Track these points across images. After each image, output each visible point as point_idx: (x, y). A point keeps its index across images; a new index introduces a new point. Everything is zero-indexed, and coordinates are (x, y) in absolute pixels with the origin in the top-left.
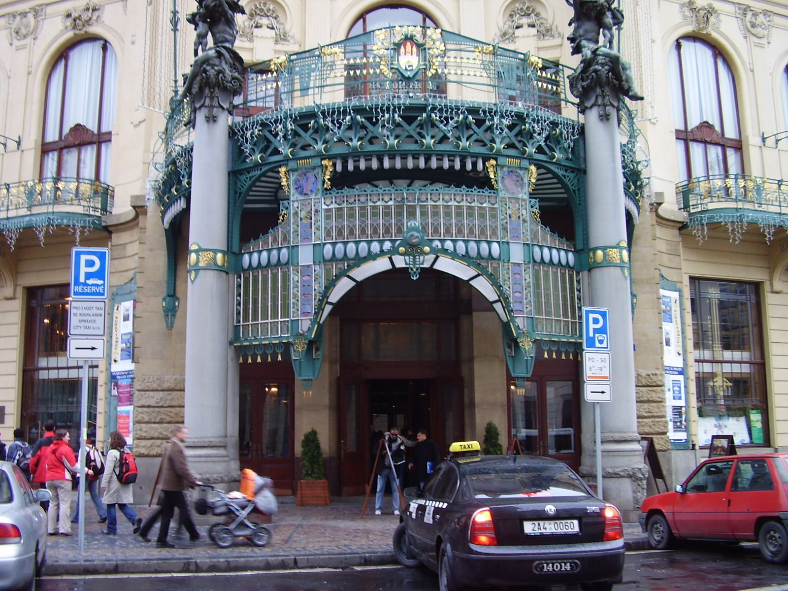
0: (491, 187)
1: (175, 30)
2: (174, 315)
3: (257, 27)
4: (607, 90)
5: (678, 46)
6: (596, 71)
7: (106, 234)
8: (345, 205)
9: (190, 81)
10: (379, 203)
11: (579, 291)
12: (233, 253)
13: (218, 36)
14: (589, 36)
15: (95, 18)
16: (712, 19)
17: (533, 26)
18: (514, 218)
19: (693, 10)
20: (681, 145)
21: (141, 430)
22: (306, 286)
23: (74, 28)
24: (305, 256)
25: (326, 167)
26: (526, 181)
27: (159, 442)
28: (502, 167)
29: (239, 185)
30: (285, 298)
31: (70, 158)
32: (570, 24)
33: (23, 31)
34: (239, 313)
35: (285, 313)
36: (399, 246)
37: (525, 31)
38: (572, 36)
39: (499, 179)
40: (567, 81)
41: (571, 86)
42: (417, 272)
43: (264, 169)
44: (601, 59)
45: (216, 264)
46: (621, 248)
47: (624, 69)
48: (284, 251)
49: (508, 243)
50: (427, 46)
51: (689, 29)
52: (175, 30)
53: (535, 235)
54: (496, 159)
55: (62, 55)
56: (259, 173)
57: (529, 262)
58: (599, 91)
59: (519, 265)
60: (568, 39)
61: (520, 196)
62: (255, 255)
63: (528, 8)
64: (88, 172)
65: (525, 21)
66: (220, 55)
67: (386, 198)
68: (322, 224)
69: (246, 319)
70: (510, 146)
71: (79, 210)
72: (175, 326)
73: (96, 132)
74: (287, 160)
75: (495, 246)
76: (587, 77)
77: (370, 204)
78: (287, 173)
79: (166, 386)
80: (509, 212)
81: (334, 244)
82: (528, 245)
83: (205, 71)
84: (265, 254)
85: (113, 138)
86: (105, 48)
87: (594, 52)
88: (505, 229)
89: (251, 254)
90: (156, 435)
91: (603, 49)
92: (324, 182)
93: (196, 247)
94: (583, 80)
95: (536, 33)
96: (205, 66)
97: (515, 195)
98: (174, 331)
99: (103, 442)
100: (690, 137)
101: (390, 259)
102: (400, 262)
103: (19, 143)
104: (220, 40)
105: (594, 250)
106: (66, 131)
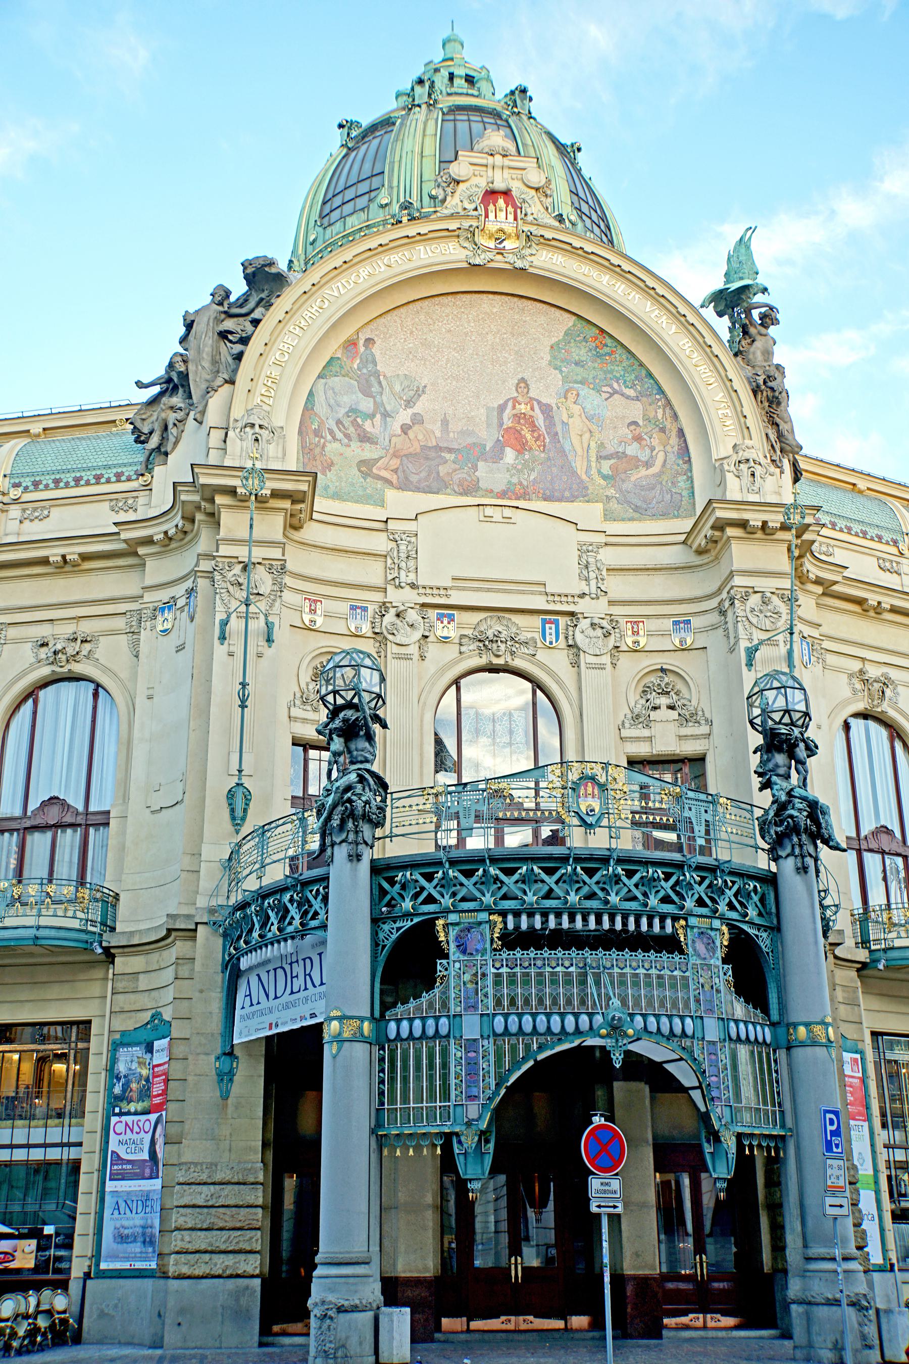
0: (682, 952)
1: (243, 706)
2: (231, 1080)
4: (804, 837)
5: (847, 727)
6: (791, 817)
8: (518, 969)
10: (558, 969)
11: (776, 1072)
12: (379, 1020)
13: (355, 753)
14: (781, 771)
15: (84, 652)
16: (888, 692)
17: (672, 708)
18: (707, 987)
19: (865, 682)
21: (182, 1240)
22: (472, 1066)
24: (471, 1027)
25: (496, 923)
26: (718, 943)
27: (207, 1257)
28: (693, 927)
29: (381, 935)
30: (445, 1077)
31: (39, 843)
32: (755, 752)
34: (381, 1093)
35: (446, 1096)
37: (664, 714)
38: (761, 770)
39: (690, 942)
40: (756, 822)
41: (762, 830)
42: (620, 1058)
43: (416, 920)
46: (827, 1025)
47: (824, 813)
48: (443, 1021)
49: (702, 1018)
50: (609, 787)
51: (860, 706)
52: (243, 706)
54: (686, 919)
55: (31, 694)
56: (409, 924)
57: (725, 1040)
58: (795, 839)
59: (714, 1043)
60: (755, 772)
61: (712, 962)
62: (405, 1024)
64: (66, 867)
65: (664, 701)
66: (361, 779)
68: (490, 991)
69: (393, 1101)
70: (700, 902)
71: (76, 924)
72: (232, 1094)
73: (81, 808)
75: (688, 1021)
76: (782, 822)
77: (548, 969)
78: (446, 926)
79: (218, 1177)
80: (701, 981)
81: (506, 1016)
82: (723, 1019)
83: (350, 801)
85: (112, 822)
86: (96, 695)
87: (789, 794)
88: (698, 1001)
89: (399, 1021)
90: (203, 1247)
91: (798, 789)
93: (339, 1014)
94: (776, 825)
95: (677, 717)
96: (349, 794)
97: (706, 963)
98: (230, 1101)
99: (91, 1259)
100: (864, 846)
102: (590, 1042)
104: (360, 759)
105: (795, 1025)
106: (33, 805)
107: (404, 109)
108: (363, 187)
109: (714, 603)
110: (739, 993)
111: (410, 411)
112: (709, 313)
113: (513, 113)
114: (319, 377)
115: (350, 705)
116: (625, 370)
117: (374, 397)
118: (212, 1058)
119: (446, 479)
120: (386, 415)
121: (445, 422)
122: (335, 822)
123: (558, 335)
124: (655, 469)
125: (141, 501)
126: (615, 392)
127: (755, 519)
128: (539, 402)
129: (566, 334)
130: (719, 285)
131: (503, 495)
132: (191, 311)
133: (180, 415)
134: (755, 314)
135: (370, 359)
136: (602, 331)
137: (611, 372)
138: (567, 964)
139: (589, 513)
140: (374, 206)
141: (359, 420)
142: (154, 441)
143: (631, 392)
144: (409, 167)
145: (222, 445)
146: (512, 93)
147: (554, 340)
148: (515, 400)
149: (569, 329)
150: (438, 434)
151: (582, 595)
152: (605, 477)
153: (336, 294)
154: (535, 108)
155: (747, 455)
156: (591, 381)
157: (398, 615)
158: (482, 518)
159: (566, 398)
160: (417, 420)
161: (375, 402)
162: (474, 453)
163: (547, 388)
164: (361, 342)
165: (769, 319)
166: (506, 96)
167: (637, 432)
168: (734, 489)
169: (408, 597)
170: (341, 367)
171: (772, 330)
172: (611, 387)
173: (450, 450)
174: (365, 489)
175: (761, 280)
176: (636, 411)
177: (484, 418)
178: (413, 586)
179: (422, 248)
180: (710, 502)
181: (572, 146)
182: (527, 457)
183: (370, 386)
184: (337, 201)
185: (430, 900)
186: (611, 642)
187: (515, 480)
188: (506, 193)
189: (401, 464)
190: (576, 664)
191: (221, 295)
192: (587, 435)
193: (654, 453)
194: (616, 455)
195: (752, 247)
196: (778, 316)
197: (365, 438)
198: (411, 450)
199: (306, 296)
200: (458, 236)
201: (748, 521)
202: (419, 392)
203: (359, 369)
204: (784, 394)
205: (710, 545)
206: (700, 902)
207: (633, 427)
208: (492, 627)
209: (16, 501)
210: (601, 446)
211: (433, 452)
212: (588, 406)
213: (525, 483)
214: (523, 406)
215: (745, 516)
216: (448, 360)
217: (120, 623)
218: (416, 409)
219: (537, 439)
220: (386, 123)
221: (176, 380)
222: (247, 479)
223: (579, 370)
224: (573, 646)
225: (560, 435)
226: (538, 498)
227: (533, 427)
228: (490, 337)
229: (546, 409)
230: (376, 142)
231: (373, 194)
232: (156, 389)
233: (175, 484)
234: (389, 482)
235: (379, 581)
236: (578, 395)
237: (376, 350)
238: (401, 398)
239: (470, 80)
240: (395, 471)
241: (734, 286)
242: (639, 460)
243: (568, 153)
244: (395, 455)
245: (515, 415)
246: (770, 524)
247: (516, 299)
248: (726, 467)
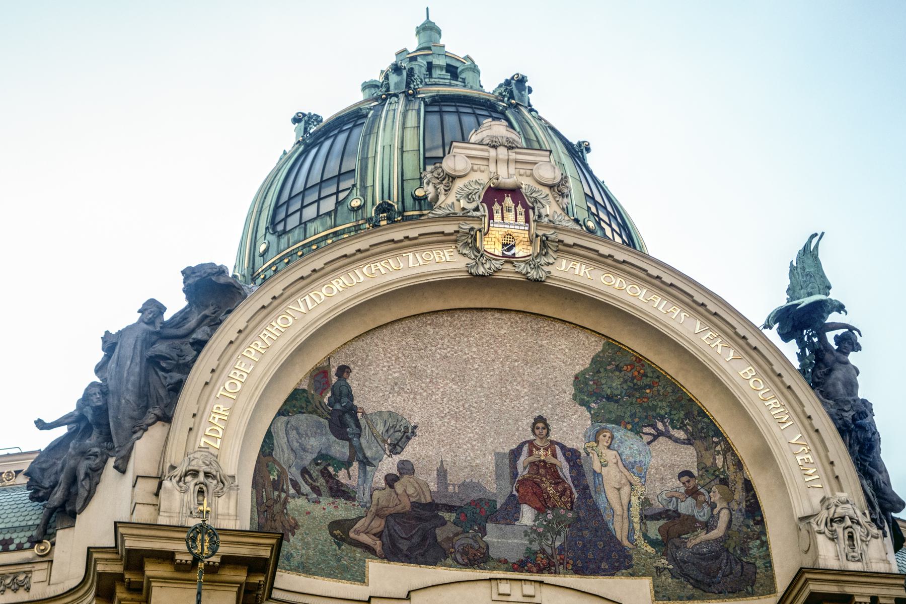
107: (376, 99)
111: (397, 458)
112: (773, 335)
113: (510, 105)
114: (281, 413)
116: (671, 406)
117: (349, 440)
119: (445, 546)
120: (365, 462)
121: (442, 473)
123: (582, 363)
124: (718, 532)
125: (39, 574)
126: (660, 434)
128: (563, 447)
129: (594, 361)
130: (781, 301)
131: (520, 566)
132: (113, 331)
133: (94, 462)
134: (830, 336)
135: (345, 391)
136: (640, 360)
137: (654, 408)
140: (343, 210)
141: (331, 469)
142: (58, 495)
143: (681, 434)
144: (386, 163)
145: (153, 500)
146: (508, 83)
147: (579, 369)
148: (531, 442)
149: (597, 355)
150: (433, 487)
152: (653, 543)
153: (303, 309)
154: (534, 99)
155: (840, 511)
156: (628, 419)
158: (495, 597)
159: (597, 441)
160: (406, 468)
161: (351, 446)
162: (478, 512)
163: (572, 427)
164: (333, 371)
165: (849, 342)
166: (500, 86)
167: (692, 484)
168: (829, 554)
170: (308, 401)
172: (654, 426)
173: (450, 508)
174: (339, 560)
175: (833, 295)
177: (492, 468)
179: (411, 255)
180: (801, 571)
181: (580, 144)
182: (550, 517)
183: (345, 425)
184: (296, 205)
187: (535, 547)
188: (515, 192)
189: (387, 525)
191: (153, 309)
192: (626, 490)
193: (715, 512)
194: (664, 514)
195: (820, 257)
196: (860, 340)
197: (339, 492)
198: (399, 508)
199: (265, 312)
200: (456, 241)
201: (850, 597)
202: (408, 433)
203: (329, 404)
204: (876, 436)
207: (685, 479)
211: (426, 513)
212: (627, 452)
213: (549, 551)
214: (542, 452)
215: (849, 590)
216: (444, 393)
219: (562, 494)
220: (353, 118)
221: (90, 417)
222: (194, 540)
223: (613, 406)
225: (592, 488)
226: (567, 572)
227: (557, 479)
228: (497, 365)
229: (572, 456)
230: (342, 138)
231: (342, 196)
232: (63, 430)
233: (89, 548)
236: (612, 437)
237: (353, 382)
238: (385, 441)
239: (452, 71)
240: (379, 535)
241: (806, 301)
242: (697, 521)
243: (577, 152)
244: (377, 515)
245: (532, 464)
246: (882, 601)
247: (529, 319)
248: (816, 528)
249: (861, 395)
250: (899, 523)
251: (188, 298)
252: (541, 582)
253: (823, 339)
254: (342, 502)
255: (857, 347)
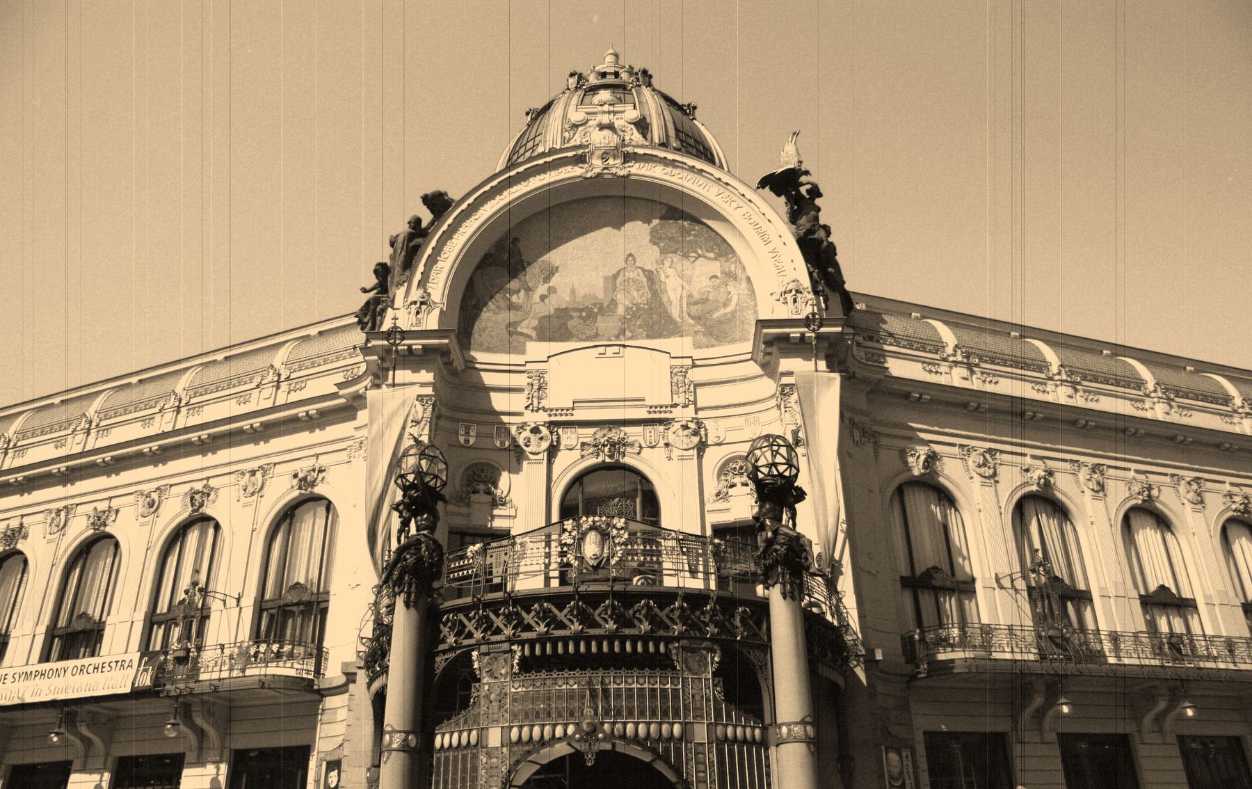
0: (674, 668)
3: (474, 492)
6: (776, 550)
7: (317, 697)
9: (390, 568)
18: (697, 697)
20: (907, 598)
23: (300, 488)
24: (494, 738)
33: (250, 489)
36: (574, 734)
44: (781, 539)
45: (408, 745)
48: (474, 733)
53: (718, 715)
56: (453, 655)
59: (702, 744)
63: (741, 468)
65: (738, 480)
67: (571, 682)
71: (292, 673)
74: (478, 644)
75: (677, 729)
83: (405, 559)
84: (456, 736)
88: (686, 707)
89: (443, 735)
92: (512, 666)
94: (765, 559)
101: (569, 744)
103: (238, 600)
105: (780, 726)
108: (530, 145)
109: (773, 402)
110: (728, 700)
114: (478, 267)
115: (413, 486)
118: (364, 770)
120: (528, 290)
121: (573, 292)
122: (395, 577)
126: (700, 256)
127: (795, 332)
128: (644, 270)
134: (803, 190)
138: (571, 682)
139: (680, 345)
143: (712, 255)
150: (567, 299)
151: (675, 405)
157: (532, 431)
165: (815, 192)
168: (783, 312)
169: (543, 417)
171: (818, 202)
173: (575, 310)
176: (715, 267)
178: (544, 409)
185: (470, 635)
186: (696, 440)
188: (611, 127)
190: (670, 459)
191: (416, 222)
197: (511, 307)
205: (768, 358)
206: (692, 626)
208: (602, 435)
209: (287, 379)
210: (690, 296)
211: (563, 313)
217: (343, 456)
218: (551, 284)
224: (667, 445)
234: (530, 338)
235: (522, 409)
237: (522, 245)
240: (535, 329)
249: (822, 222)
250: (852, 296)
251: (432, 212)
252: (624, 346)
253: (798, 192)
254: (512, 313)
255: (820, 195)
